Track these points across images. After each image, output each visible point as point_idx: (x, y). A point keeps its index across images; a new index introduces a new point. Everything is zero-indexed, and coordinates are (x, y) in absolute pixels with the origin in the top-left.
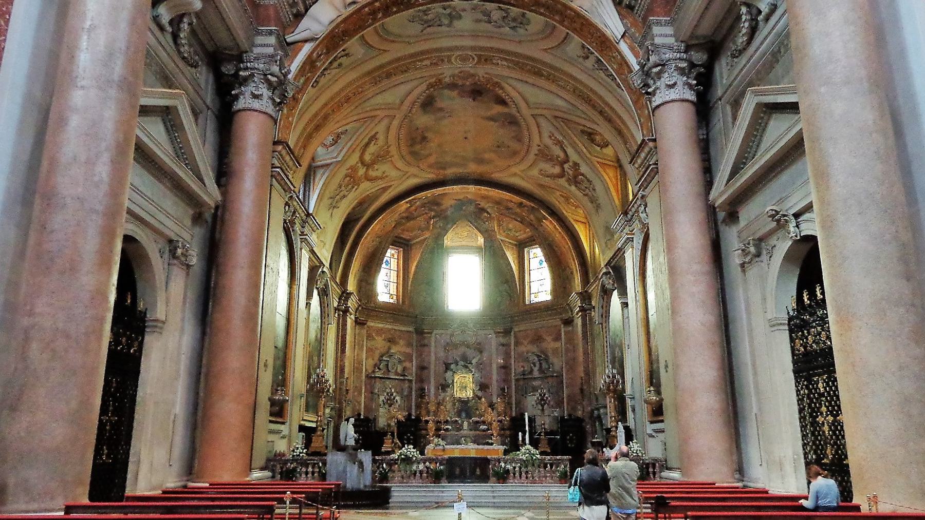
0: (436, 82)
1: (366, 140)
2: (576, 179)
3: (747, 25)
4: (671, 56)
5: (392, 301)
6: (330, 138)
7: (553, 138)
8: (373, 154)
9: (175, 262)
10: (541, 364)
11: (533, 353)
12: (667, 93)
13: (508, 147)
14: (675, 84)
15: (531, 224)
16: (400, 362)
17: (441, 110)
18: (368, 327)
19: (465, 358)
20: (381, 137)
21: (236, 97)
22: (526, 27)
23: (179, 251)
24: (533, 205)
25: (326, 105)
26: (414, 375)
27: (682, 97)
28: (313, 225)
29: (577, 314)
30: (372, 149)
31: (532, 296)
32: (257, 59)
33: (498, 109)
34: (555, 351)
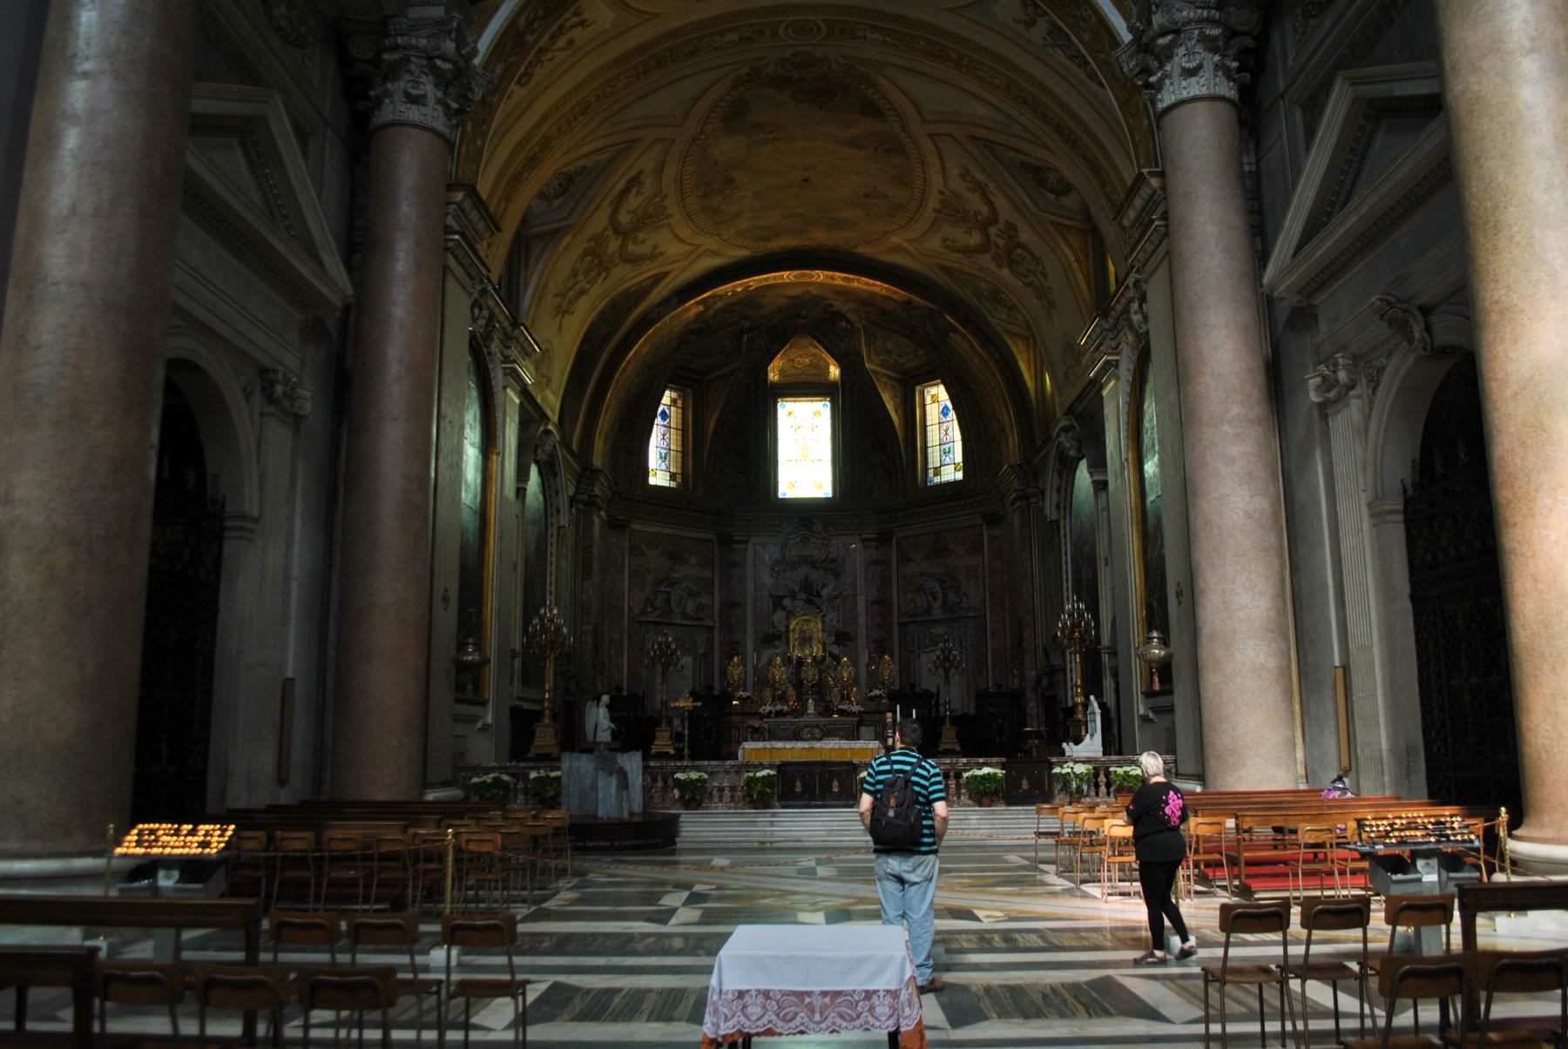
0: (748, 74)
1: (621, 185)
4: (1192, 15)
5: (673, 484)
7: (967, 178)
8: (634, 212)
9: (272, 409)
12: (1184, 84)
13: (886, 196)
14: (1200, 67)
16: (692, 595)
19: (807, 586)
20: (649, 181)
21: (378, 103)
23: (279, 389)
24: (930, 305)
25: (544, 119)
26: (717, 618)
27: (1212, 91)
28: (526, 344)
30: (633, 202)
31: (931, 473)
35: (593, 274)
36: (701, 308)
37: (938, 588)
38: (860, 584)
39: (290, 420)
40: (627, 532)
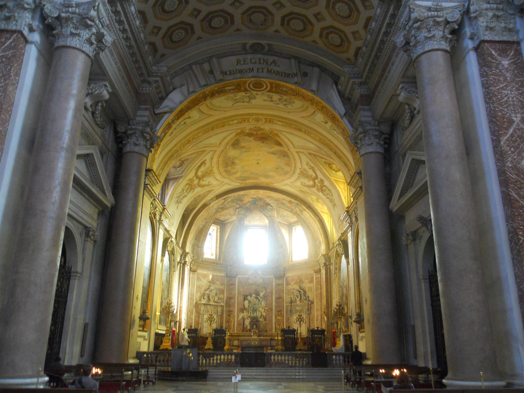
0: (240, 132)
1: (199, 164)
2: (322, 188)
3: (409, 114)
6: (178, 163)
8: (203, 172)
10: (301, 297)
11: (297, 290)
12: (368, 148)
13: (283, 169)
14: (372, 143)
15: (297, 213)
17: (244, 147)
18: (197, 273)
21: (126, 144)
22: (293, 104)
23: (91, 233)
24: (297, 202)
25: (176, 145)
28: (166, 215)
29: (323, 267)
30: (203, 169)
32: (138, 123)
33: (277, 148)
34: (310, 289)
35: (189, 190)
36: (223, 201)
37: (298, 294)
38: (274, 292)
39: (93, 242)
40: (196, 273)
